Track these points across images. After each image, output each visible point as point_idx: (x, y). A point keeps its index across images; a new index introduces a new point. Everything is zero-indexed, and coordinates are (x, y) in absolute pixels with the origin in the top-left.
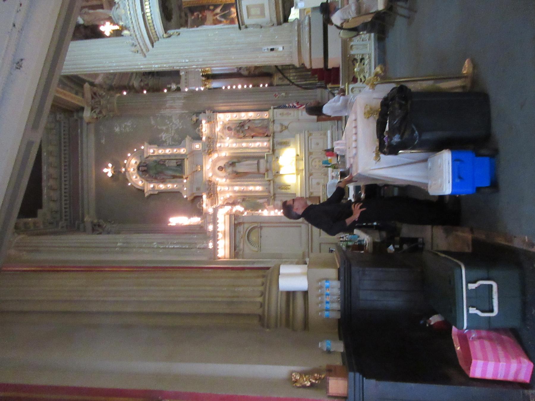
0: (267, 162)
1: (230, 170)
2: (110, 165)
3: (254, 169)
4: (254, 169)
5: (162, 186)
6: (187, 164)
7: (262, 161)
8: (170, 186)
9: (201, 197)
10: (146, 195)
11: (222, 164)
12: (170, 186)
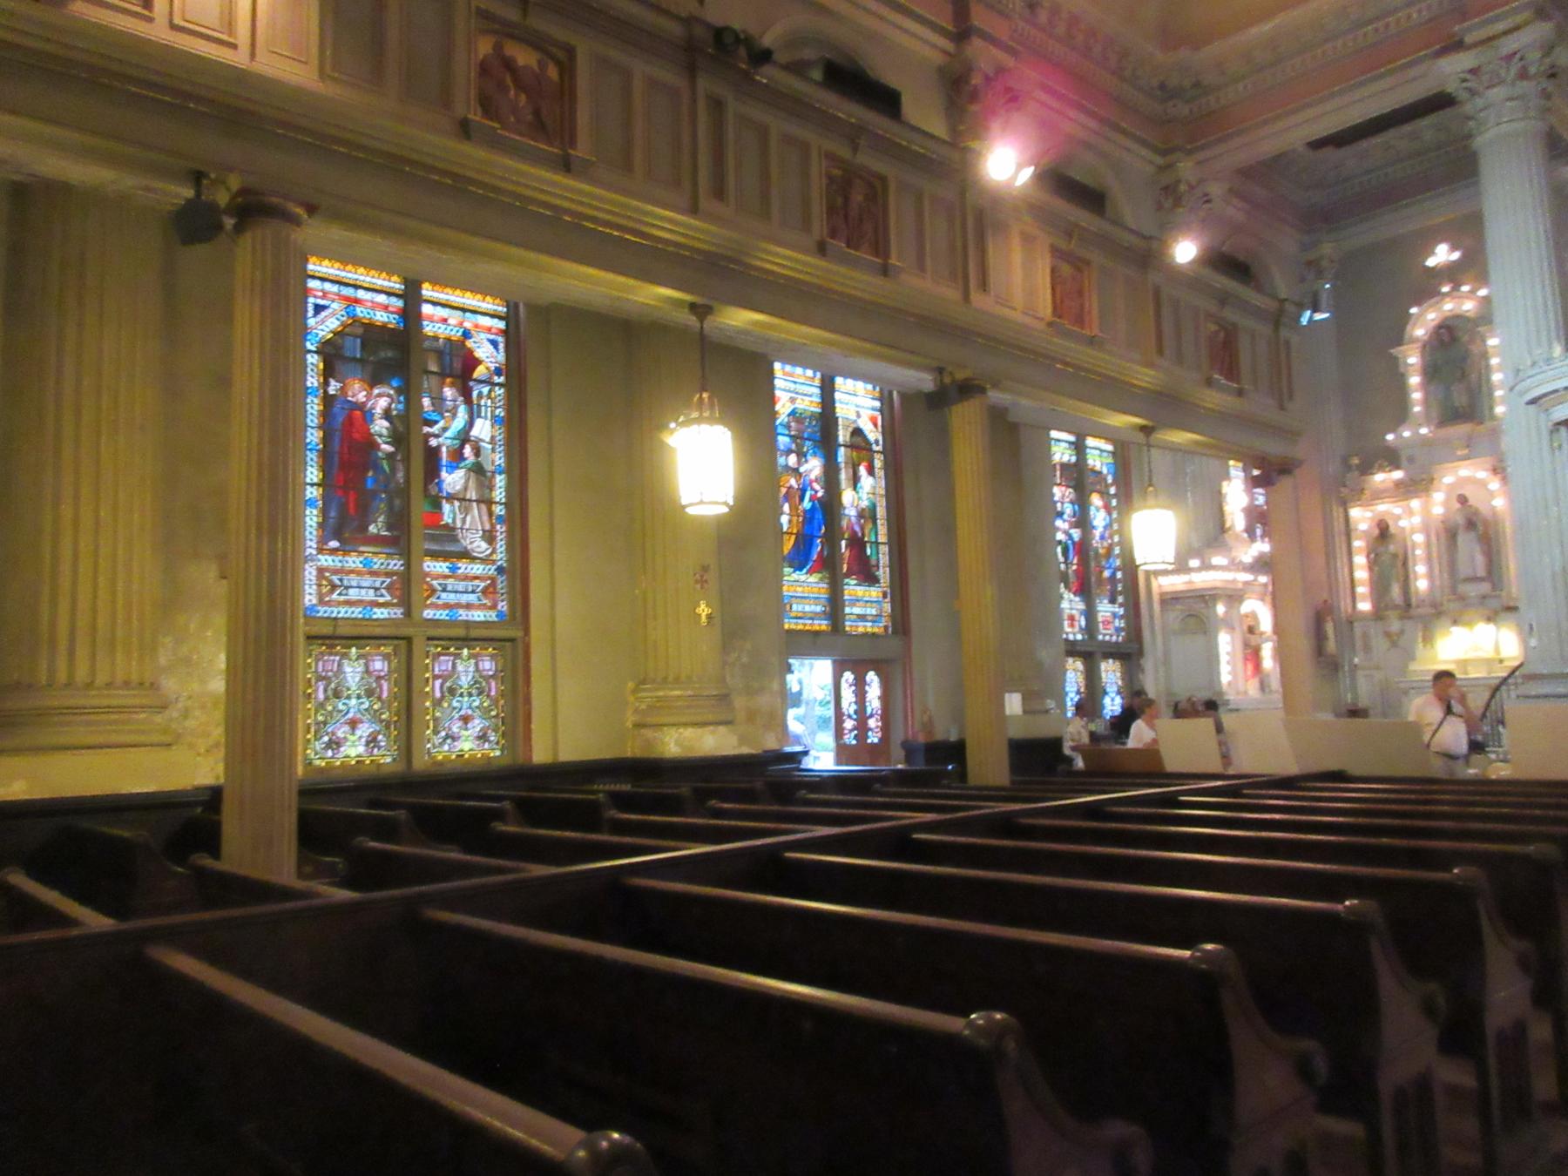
0: (1484, 597)
1: (1460, 520)
2: (1456, 256)
3: (1464, 570)
4: (1464, 570)
5: (1414, 380)
6: (1463, 429)
7: (1485, 587)
8: (1417, 396)
9: (1398, 467)
10: (1393, 351)
11: (1475, 500)
12: (1417, 396)
